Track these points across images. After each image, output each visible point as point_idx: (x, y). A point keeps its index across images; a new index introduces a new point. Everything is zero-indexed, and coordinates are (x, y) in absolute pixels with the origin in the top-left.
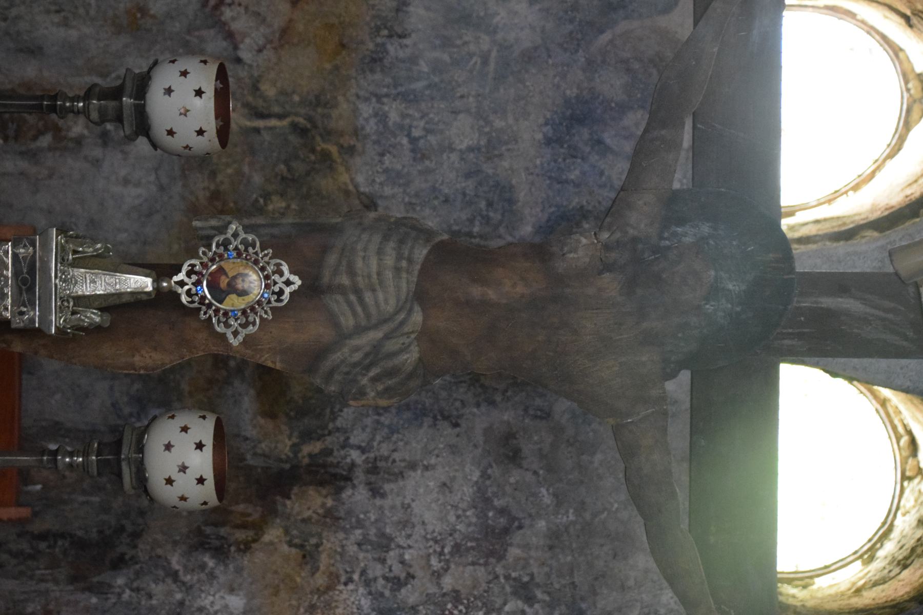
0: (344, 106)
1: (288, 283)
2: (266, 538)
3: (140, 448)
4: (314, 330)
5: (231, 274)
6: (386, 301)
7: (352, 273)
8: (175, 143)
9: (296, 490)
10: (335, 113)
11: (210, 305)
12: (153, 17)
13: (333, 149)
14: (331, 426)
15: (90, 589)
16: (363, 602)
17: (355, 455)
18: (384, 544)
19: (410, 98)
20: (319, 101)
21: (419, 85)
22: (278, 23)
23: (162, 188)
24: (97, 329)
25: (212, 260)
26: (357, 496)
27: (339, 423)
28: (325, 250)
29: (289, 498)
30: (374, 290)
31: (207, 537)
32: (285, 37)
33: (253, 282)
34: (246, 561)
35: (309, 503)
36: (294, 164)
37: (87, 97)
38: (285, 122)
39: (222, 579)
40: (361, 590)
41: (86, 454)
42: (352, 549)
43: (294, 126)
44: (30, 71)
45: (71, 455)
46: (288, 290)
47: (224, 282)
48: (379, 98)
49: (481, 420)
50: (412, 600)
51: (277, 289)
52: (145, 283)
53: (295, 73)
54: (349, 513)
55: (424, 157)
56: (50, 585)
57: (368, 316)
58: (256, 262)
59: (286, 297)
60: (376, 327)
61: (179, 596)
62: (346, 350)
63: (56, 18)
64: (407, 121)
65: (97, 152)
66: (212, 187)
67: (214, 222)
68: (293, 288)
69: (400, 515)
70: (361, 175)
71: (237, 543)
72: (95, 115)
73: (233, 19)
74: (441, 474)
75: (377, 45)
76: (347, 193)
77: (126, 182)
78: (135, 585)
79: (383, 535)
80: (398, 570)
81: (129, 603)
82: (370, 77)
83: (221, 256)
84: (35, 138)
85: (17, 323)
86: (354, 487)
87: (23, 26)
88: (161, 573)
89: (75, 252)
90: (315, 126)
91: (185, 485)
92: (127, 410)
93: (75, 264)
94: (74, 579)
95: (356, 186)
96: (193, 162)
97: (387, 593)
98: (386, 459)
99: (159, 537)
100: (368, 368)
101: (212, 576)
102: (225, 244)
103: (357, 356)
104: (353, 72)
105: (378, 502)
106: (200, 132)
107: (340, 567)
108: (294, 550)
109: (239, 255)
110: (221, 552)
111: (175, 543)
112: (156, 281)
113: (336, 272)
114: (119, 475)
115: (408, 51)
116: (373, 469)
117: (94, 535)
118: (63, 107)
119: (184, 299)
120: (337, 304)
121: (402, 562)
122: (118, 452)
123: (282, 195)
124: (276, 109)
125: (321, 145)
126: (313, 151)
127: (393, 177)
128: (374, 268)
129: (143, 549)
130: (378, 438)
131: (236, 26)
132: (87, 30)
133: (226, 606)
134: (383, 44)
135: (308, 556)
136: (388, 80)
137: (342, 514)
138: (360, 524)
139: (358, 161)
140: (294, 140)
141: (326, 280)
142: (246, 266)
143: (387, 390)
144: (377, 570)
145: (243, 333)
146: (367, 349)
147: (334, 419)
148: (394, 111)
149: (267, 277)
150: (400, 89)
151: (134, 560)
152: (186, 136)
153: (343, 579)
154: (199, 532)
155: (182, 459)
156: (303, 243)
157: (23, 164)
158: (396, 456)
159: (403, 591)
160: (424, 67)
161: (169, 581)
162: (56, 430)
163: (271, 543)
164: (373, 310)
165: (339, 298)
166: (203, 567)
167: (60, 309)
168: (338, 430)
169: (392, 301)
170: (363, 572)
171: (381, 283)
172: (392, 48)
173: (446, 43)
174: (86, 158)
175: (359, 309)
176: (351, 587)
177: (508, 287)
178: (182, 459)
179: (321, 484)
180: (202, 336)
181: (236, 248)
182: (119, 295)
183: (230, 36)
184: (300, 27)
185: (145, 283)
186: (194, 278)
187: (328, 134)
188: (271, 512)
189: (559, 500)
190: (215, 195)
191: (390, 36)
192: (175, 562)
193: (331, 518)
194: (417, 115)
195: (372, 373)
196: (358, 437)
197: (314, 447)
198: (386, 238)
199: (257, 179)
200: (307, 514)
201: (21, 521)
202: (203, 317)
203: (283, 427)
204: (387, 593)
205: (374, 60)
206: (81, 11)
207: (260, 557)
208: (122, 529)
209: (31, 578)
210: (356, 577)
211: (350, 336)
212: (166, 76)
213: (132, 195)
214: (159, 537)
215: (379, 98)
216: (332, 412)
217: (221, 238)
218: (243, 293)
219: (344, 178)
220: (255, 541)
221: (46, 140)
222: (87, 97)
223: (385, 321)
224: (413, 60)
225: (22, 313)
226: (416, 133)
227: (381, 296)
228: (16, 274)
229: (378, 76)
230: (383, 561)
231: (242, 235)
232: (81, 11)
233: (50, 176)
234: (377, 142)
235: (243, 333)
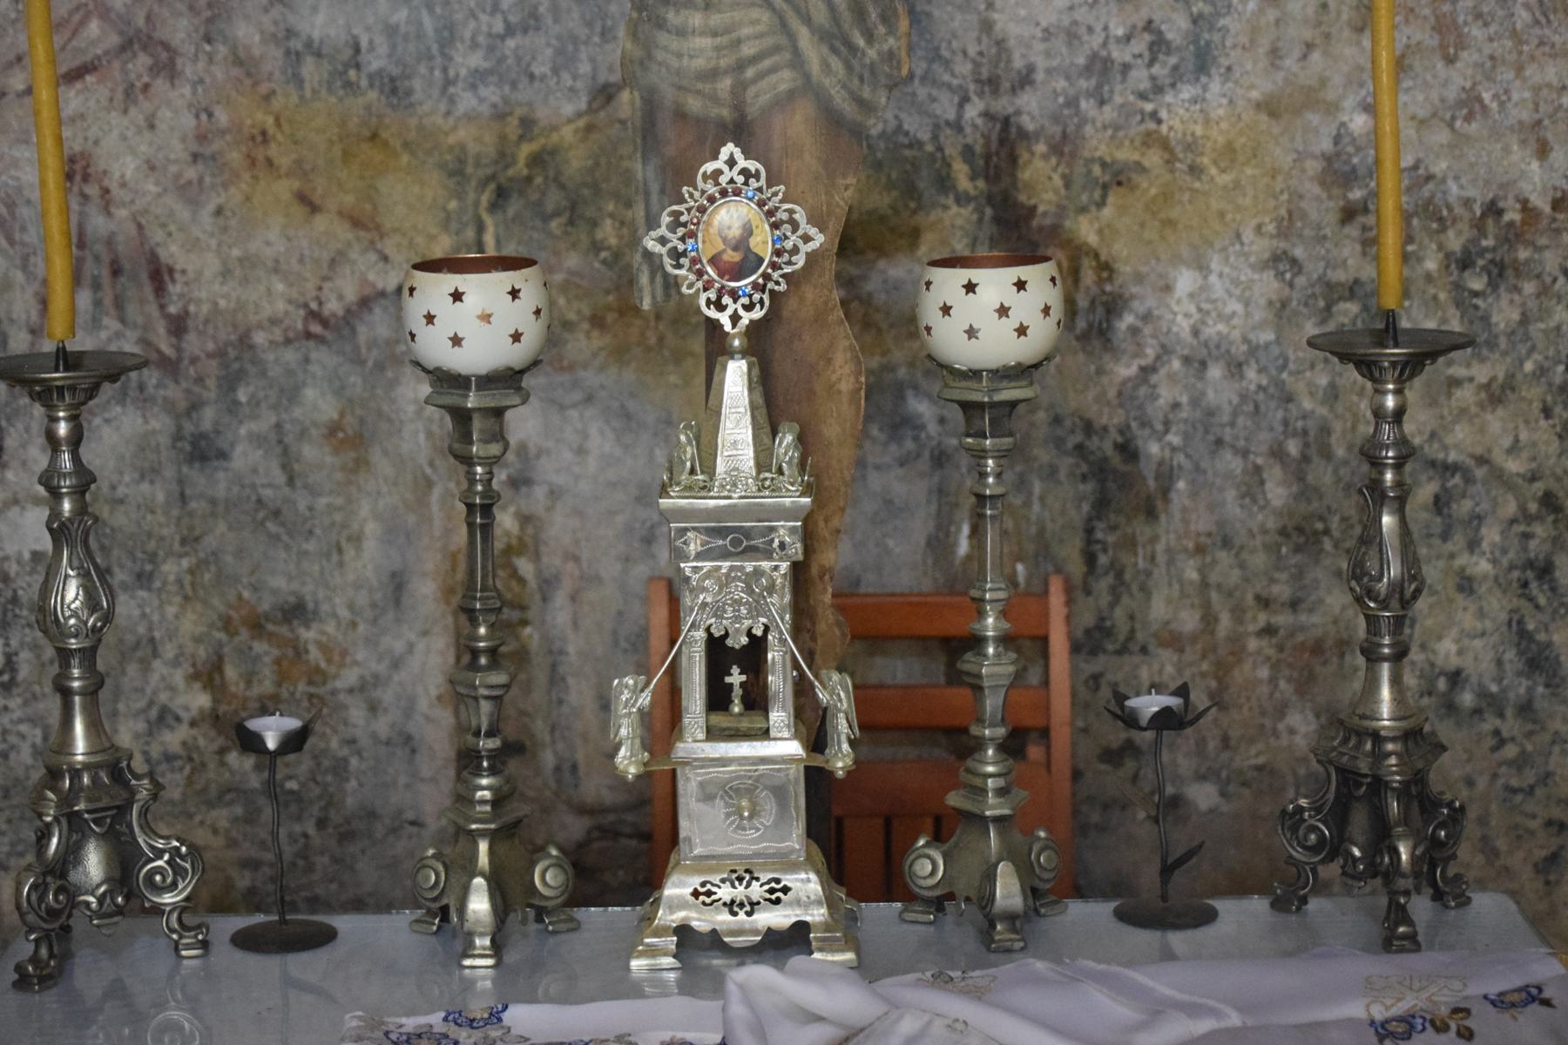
0: (463, 134)
1: (731, 162)
2: (1092, 239)
3: (974, 374)
4: (798, 125)
5: (722, 247)
6: (757, 22)
7: (713, 74)
8: (533, 332)
9: (1022, 198)
10: (473, 148)
11: (766, 277)
12: (342, 414)
13: (526, 150)
14: (929, 148)
15: (1165, 492)
16: (1185, 95)
17: (972, 112)
18: (1101, 68)
19: (448, 36)
20: (456, 171)
21: (428, 24)
22: (344, 232)
23: (589, 399)
24: (801, 440)
25: (700, 273)
26: (1031, 108)
27: (925, 136)
28: (681, 115)
29: (1034, 208)
30: (739, 42)
31: (1091, 326)
32: (362, 222)
33: (731, 217)
34: (1125, 269)
36: (550, 207)
37: (467, 461)
38: (489, 221)
39: (1151, 302)
40: (1169, 98)
41: (981, 454)
42: (1108, 113)
43: (494, 207)
44: (426, 590)
45: (983, 475)
46: (742, 163)
47: (732, 257)
48: (448, 82)
50: (1183, 23)
51: (740, 179)
52: (736, 376)
53: (414, 203)
54: (1056, 119)
55: (534, 15)
56: (1160, 547)
57: (777, 49)
58: (702, 210)
59: (753, 165)
60: (792, 38)
61: (1176, 364)
62: (827, 81)
63: (350, 553)
64: (481, 39)
65: (540, 492)
66: (586, 326)
67: (644, 279)
68: (738, 155)
69: (1059, 44)
70: (561, 108)
71: (1100, 282)
72: (494, 449)
73: (341, 298)
75: (371, 86)
76: (590, 128)
77: (581, 451)
78: (1159, 427)
79: (1088, 70)
80: (1140, 45)
81: (1186, 437)
82: (418, 96)
83: (694, 261)
84: (522, 581)
85: (796, 550)
86: (1018, 113)
87: (362, 599)
88: (1143, 391)
89: (692, 471)
90: (493, 177)
91: (1027, 307)
92: (909, 445)
93: (710, 471)
94: (1151, 514)
95: (579, 115)
96: (556, 331)
97: (1173, 60)
98: (977, 65)
99: (1091, 395)
100: (853, 48)
101: (1147, 317)
102: (676, 255)
103: (837, 65)
104: (413, 122)
105: (1039, 76)
106: (514, 293)
107: (1136, 129)
108: (1111, 199)
109: (692, 235)
110: (1113, 306)
111: (1100, 371)
112: (730, 354)
113: (714, 98)
114: (1013, 404)
115: (380, 40)
116: (991, 85)
117: (1088, 488)
118: (484, 495)
119: (757, 314)
120: (760, 96)
121: (1128, 38)
122: (980, 406)
123: (594, 224)
124: (470, 234)
125: (520, 168)
126: (529, 179)
127: (564, 59)
128: (706, 42)
129: (1111, 418)
130: (946, 78)
131: (351, 294)
132: (365, 509)
133: (1191, 296)
134: (370, 77)
135: (1118, 178)
136: (422, 69)
137: (1057, 130)
138: (1072, 103)
139: (542, 114)
140: (514, 206)
141: (725, 113)
142: (709, 224)
143: (884, 19)
144: (1140, 77)
145: (804, 227)
146: (825, 50)
147: (917, 144)
148: (468, 60)
149: (724, 193)
150: (435, 48)
151: (1124, 430)
152: (520, 315)
153: (1152, 126)
154: (1084, 337)
155: (988, 315)
156: (668, 142)
157: (560, 598)
158: (972, 50)
159: (1170, 36)
160: (401, 15)
161: (1154, 379)
162: (940, 543)
163: (1100, 232)
164: (769, 42)
165: (751, 91)
166: (1134, 331)
167: (775, 490)
168: (935, 137)
169: (755, 13)
170: (1143, 96)
171: (728, 30)
172: (375, 63)
174: (549, 509)
175: (767, 63)
176: (1163, 114)
178: (988, 315)
179: (1013, 160)
180: (809, 293)
181: (682, 239)
182: (753, 407)
183: (365, 303)
184: (349, 199)
185: (736, 376)
186: (726, 300)
187: (504, 157)
190: (597, 322)
191: (358, 66)
192: (1125, 370)
193: (1064, 146)
194: (472, 25)
195: (861, 43)
196: (946, 108)
197: (960, 170)
198: (661, 24)
199: (573, 261)
200: (1058, 181)
201: (1069, 590)
202: (783, 287)
203: (933, 217)
204: (1173, 60)
205: (394, 91)
206: (338, 517)
207: (1122, 252)
208: (1079, 448)
209: (1148, 574)
210: (1149, 107)
211: (807, 76)
212: (434, 347)
213: (601, 441)
214: (1091, 395)
215: (448, 82)
216: (910, 146)
217: (668, 262)
218: (748, 231)
219: (567, 133)
220: (1097, 256)
221: (525, 566)
222: (467, 461)
223: (784, 24)
224: (392, 31)
225: (782, 546)
226: (499, 27)
227: (746, 31)
228: (725, 555)
229: (417, 84)
230: (1126, 68)
231: (663, 231)
232: (338, 517)
233: (576, 559)
234: (514, 85)
235: (804, 227)
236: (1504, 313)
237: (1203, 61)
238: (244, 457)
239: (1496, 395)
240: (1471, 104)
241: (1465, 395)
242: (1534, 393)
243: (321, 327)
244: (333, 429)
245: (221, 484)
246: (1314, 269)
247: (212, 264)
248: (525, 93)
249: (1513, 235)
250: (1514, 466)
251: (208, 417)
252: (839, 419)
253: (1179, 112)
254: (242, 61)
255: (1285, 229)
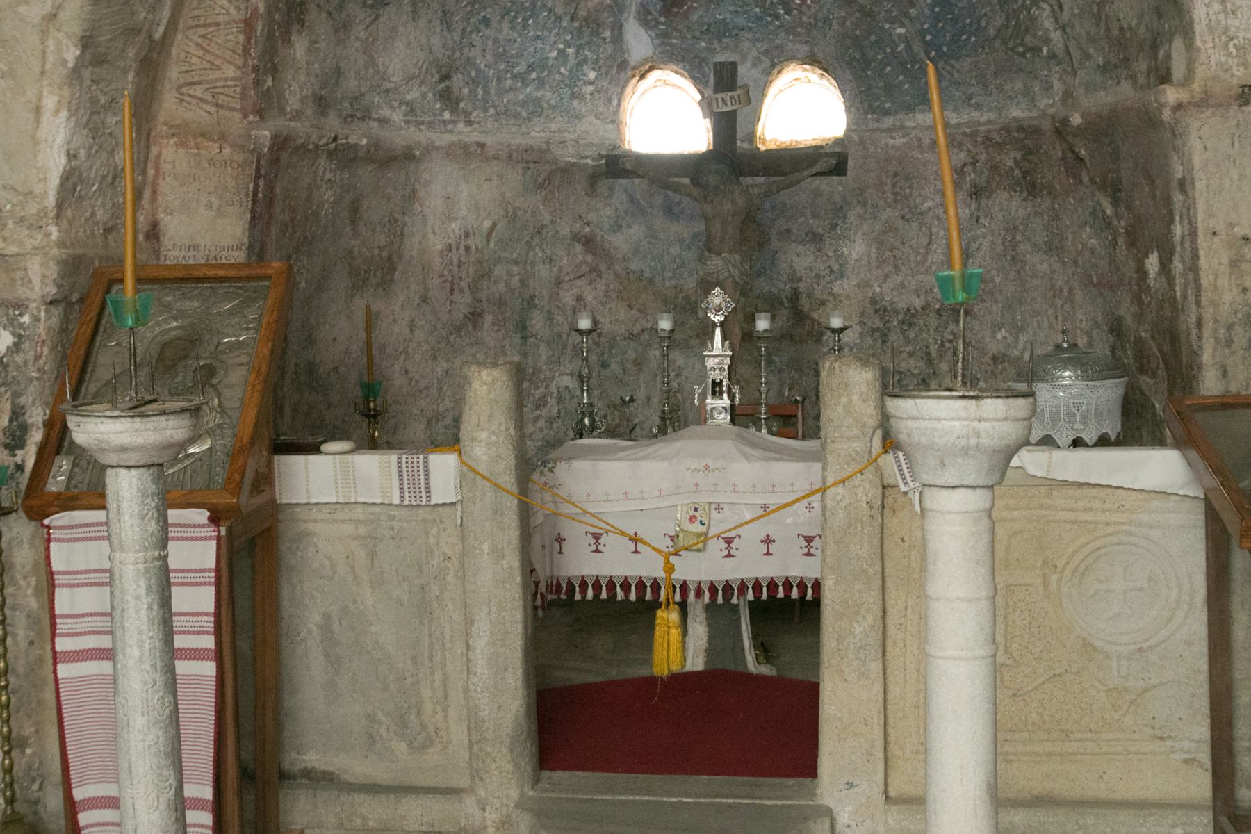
18: (818, 276)
22: (638, 314)
26: (802, 286)
35: (804, 303)
44: (655, 400)
49: (775, 244)
74: (794, 257)
116: (792, 280)
144: (827, 279)
172: (647, 275)
173: (645, 257)
177: (717, 228)
188: (808, 316)
189: (803, 215)
193: (809, 296)
196: (781, 286)
221: (679, 396)
236: (912, 335)
237: (842, 275)
238: (613, 366)
239: (911, 354)
240: (902, 285)
241: (904, 355)
242: (919, 354)
243: (632, 336)
244: (634, 361)
245: (607, 372)
246: (869, 325)
247: (608, 321)
248: (682, 282)
249: (913, 316)
250: (916, 372)
251: (606, 357)
252: (737, 340)
253: (837, 288)
254: (617, 275)
255: (862, 314)
